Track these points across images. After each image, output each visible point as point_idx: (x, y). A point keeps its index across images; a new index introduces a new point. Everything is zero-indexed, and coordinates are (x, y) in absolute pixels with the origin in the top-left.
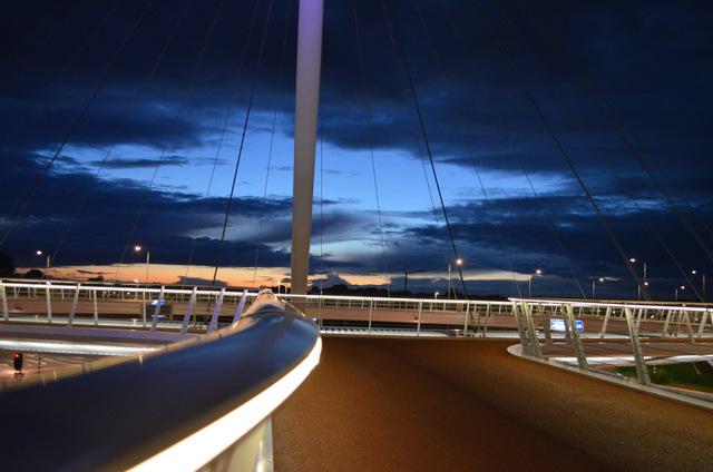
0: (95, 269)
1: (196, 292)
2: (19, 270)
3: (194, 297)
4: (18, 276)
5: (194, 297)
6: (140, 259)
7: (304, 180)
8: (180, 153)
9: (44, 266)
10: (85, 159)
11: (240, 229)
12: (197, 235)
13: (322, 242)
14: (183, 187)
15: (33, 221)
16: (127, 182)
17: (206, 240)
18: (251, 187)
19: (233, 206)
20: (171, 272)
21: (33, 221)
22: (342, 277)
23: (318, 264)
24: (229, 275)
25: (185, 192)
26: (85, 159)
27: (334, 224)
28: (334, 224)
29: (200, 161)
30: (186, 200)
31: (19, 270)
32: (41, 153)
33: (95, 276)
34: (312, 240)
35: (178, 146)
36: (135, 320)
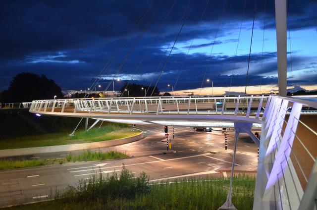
0: (190, 91)
1: (112, 100)
2: (161, 93)
3: (224, 100)
4: (161, 95)
5: (224, 100)
6: (209, 85)
7: (282, 43)
8: (217, 39)
9: (171, 91)
10: (181, 48)
11: (242, 70)
12: (229, 74)
13: (292, 70)
14: (221, 54)
15: (164, 74)
16: (198, 54)
17: (226, 76)
18: (257, 50)
19: (249, 59)
20: (221, 90)
21: (164, 74)
22: (301, 87)
23: (290, 83)
24: (251, 90)
25: (221, 55)
26: (181, 48)
27: (294, 62)
28: (294, 62)
29: (227, 41)
30: (222, 59)
31: (161, 93)
32: (163, 47)
33: (191, 94)
34: (288, 69)
35: (216, 37)
36: (209, 111)
